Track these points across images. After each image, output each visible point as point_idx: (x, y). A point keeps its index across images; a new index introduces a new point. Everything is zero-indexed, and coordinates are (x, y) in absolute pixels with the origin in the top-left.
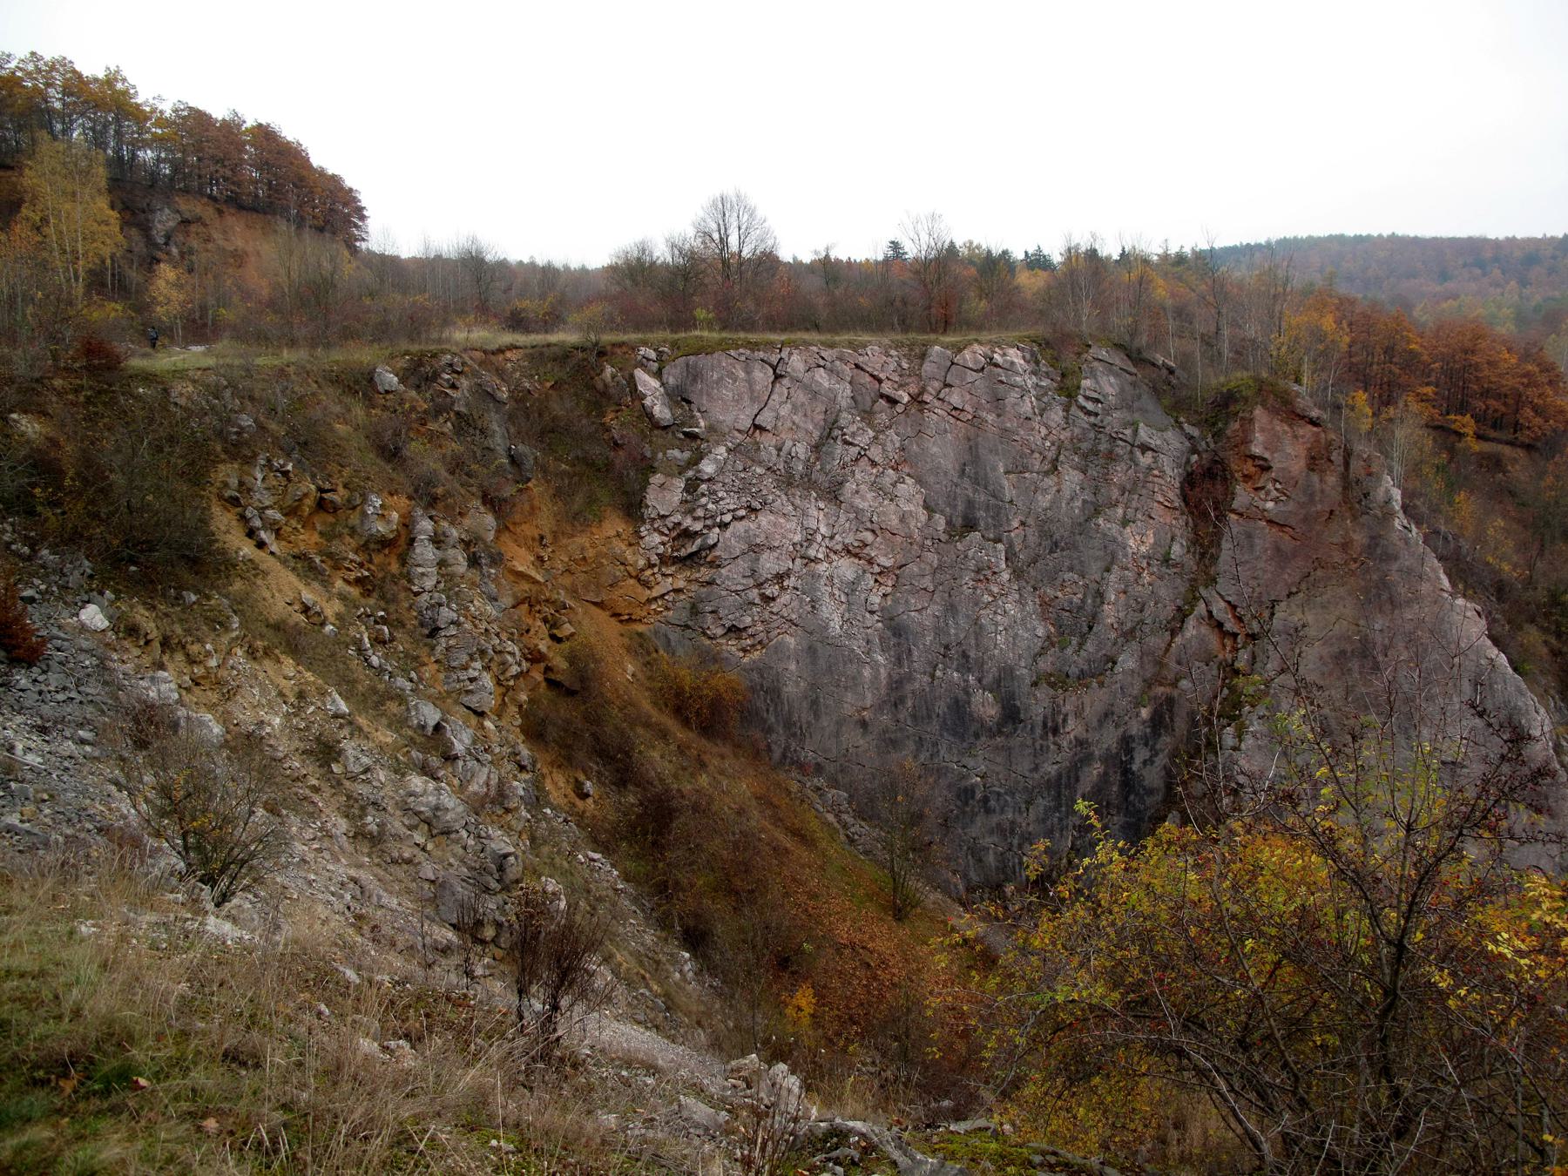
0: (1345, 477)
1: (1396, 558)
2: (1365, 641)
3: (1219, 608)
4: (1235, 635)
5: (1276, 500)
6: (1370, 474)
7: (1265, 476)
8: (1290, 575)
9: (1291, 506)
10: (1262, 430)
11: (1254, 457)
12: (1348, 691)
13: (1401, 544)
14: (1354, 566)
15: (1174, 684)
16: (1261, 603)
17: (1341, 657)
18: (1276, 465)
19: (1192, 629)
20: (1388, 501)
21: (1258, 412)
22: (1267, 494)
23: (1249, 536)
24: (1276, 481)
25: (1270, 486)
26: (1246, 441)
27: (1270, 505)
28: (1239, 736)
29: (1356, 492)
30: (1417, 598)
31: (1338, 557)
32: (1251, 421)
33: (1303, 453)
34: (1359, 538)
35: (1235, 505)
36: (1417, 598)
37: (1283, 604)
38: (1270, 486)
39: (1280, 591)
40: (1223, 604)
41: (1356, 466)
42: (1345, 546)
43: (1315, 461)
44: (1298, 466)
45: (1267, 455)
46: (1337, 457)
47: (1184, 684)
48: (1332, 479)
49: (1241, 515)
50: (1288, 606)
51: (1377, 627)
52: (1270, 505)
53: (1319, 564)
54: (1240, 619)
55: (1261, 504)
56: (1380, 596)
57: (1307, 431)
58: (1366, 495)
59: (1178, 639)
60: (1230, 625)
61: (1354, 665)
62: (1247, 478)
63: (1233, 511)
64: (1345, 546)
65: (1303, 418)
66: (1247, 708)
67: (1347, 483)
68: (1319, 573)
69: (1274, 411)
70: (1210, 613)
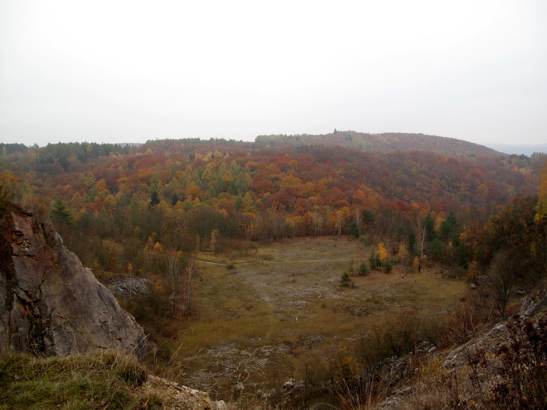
0: (44, 234)
1: (67, 259)
2: (69, 290)
3: (22, 295)
4: (29, 304)
5: (28, 247)
6: (51, 231)
7: (22, 238)
8: (41, 275)
9: (34, 248)
10: (16, 221)
11: (16, 232)
12: (71, 309)
13: (66, 253)
14: (57, 265)
15: (17, 330)
16: (36, 288)
17: (64, 299)
18: (24, 233)
19: (16, 306)
20: (59, 240)
21: (13, 214)
22: (24, 245)
23: (23, 263)
24: (26, 239)
25: (25, 242)
26: (12, 226)
27: (26, 249)
28: (51, 339)
29: (49, 239)
30: (76, 271)
31: (51, 263)
32: (11, 217)
33: (30, 227)
34: (55, 255)
35: (14, 252)
36: (76, 271)
37: (42, 286)
38: (25, 242)
39: (40, 281)
40: (23, 292)
41: (47, 229)
42: (52, 259)
43: (35, 229)
44: (30, 232)
45: (21, 230)
46: (40, 227)
47: (20, 329)
48: (42, 235)
49: (17, 255)
51: (70, 284)
52: (26, 249)
53: (47, 267)
54: (30, 296)
55: (22, 249)
56: (67, 274)
57: (29, 219)
58: (53, 239)
59: (12, 312)
60: (28, 300)
61: (69, 300)
62: (13, 240)
63: (15, 255)
64: (52, 259)
65: (25, 214)
66: (47, 329)
67: (46, 236)
68: (48, 271)
69: (16, 213)
70: (19, 298)
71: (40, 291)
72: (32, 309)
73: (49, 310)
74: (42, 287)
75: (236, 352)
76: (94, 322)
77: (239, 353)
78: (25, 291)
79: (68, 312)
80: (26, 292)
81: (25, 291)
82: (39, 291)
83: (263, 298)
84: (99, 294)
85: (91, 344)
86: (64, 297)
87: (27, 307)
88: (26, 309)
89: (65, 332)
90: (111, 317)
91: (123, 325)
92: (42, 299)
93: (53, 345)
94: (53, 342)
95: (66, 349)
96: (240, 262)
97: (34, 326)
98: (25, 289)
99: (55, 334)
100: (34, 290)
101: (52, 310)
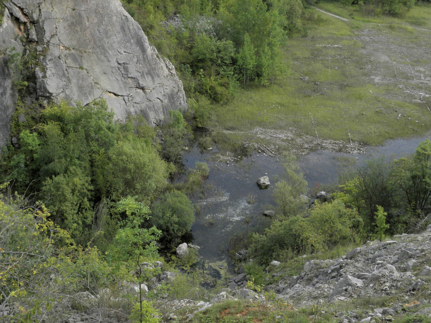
4: (25, 23)
28: (44, 70)
37: (43, 4)
40: (17, 9)
50: (45, 4)
51: (83, 9)
54: (25, 15)
60: (23, 19)
70: (11, 14)
71: (40, 10)
72: (27, 30)
73: (47, 35)
74: (43, 6)
75: (289, 138)
76: (109, 61)
77: (292, 140)
78: (19, 7)
79: (74, 43)
80: (22, 9)
81: (19, 7)
82: (37, 11)
83: (372, 77)
84: (123, 28)
85: (99, 86)
86: (73, 23)
87: (22, 27)
88: (20, 29)
89: (65, 65)
90: (135, 60)
91: (152, 73)
92: (40, 20)
93: (45, 77)
94: (45, 72)
95: (61, 86)
96: (375, 21)
97: (28, 51)
98: (19, 5)
99: (50, 65)
100: (32, 8)
101: (52, 36)
